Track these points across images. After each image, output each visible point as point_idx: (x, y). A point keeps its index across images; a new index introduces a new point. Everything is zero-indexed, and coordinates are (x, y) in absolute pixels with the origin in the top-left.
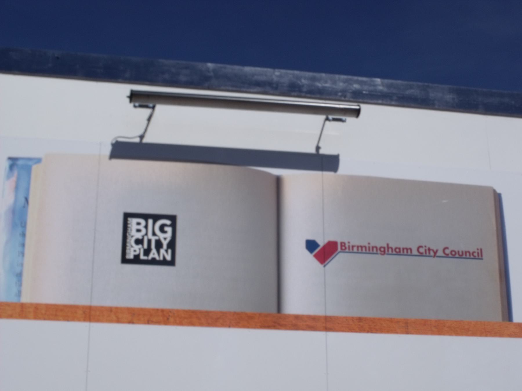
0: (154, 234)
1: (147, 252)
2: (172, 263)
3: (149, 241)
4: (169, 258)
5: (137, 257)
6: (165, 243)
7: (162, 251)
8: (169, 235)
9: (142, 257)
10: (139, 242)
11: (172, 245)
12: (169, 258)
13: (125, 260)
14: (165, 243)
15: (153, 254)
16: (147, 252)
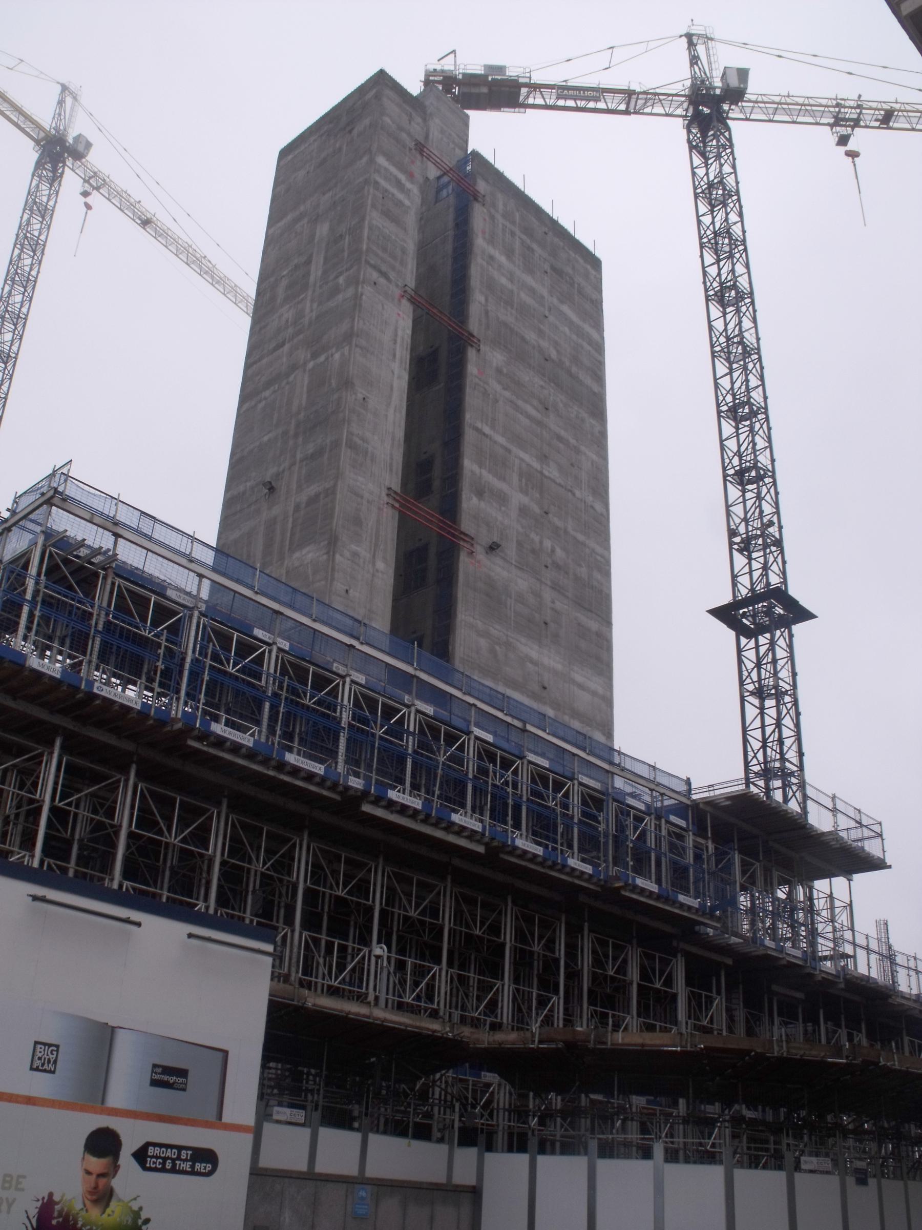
0: (48, 1055)
1: (43, 1065)
2: (53, 1072)
3: (45, 1059)
4: (53, 1069)
5: (38, 1067)
6: (52, 1061)
7: (50, 1065)
8: (54, 1056)
9: (40, 1068)
10: (40, 1059)
11: (55, 1062)
12: (53, 1069)
13: (32, 1069)
14: (52, 1061)
15: (46, 1067)
16: (43, 1065)
